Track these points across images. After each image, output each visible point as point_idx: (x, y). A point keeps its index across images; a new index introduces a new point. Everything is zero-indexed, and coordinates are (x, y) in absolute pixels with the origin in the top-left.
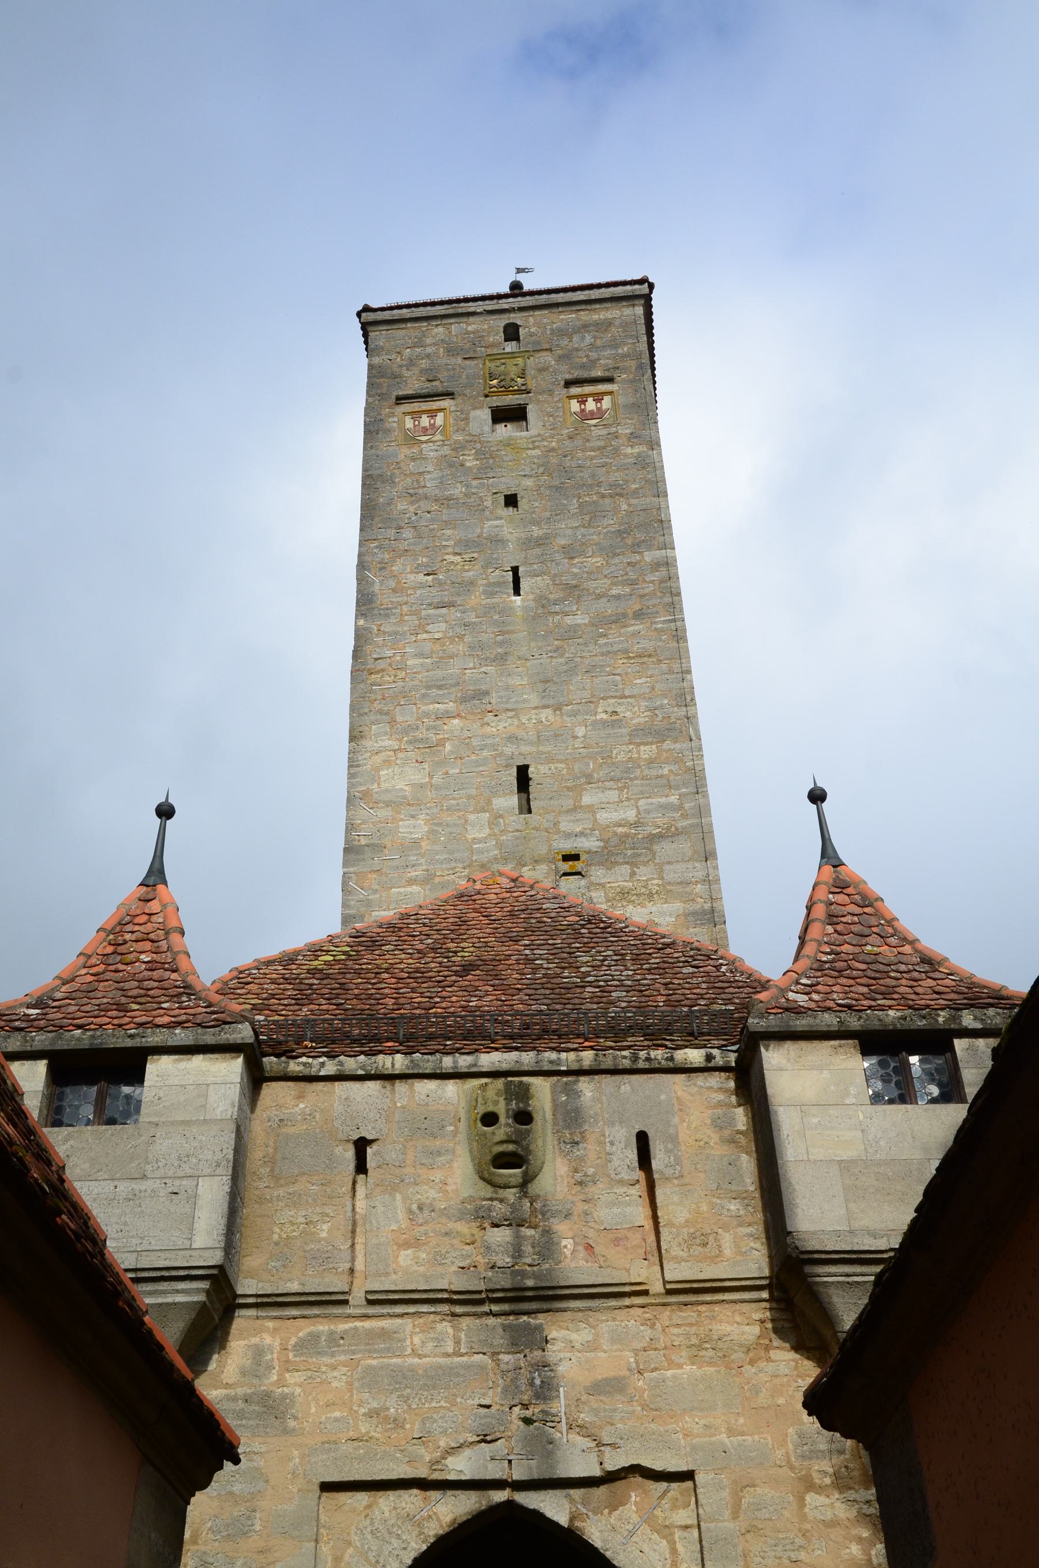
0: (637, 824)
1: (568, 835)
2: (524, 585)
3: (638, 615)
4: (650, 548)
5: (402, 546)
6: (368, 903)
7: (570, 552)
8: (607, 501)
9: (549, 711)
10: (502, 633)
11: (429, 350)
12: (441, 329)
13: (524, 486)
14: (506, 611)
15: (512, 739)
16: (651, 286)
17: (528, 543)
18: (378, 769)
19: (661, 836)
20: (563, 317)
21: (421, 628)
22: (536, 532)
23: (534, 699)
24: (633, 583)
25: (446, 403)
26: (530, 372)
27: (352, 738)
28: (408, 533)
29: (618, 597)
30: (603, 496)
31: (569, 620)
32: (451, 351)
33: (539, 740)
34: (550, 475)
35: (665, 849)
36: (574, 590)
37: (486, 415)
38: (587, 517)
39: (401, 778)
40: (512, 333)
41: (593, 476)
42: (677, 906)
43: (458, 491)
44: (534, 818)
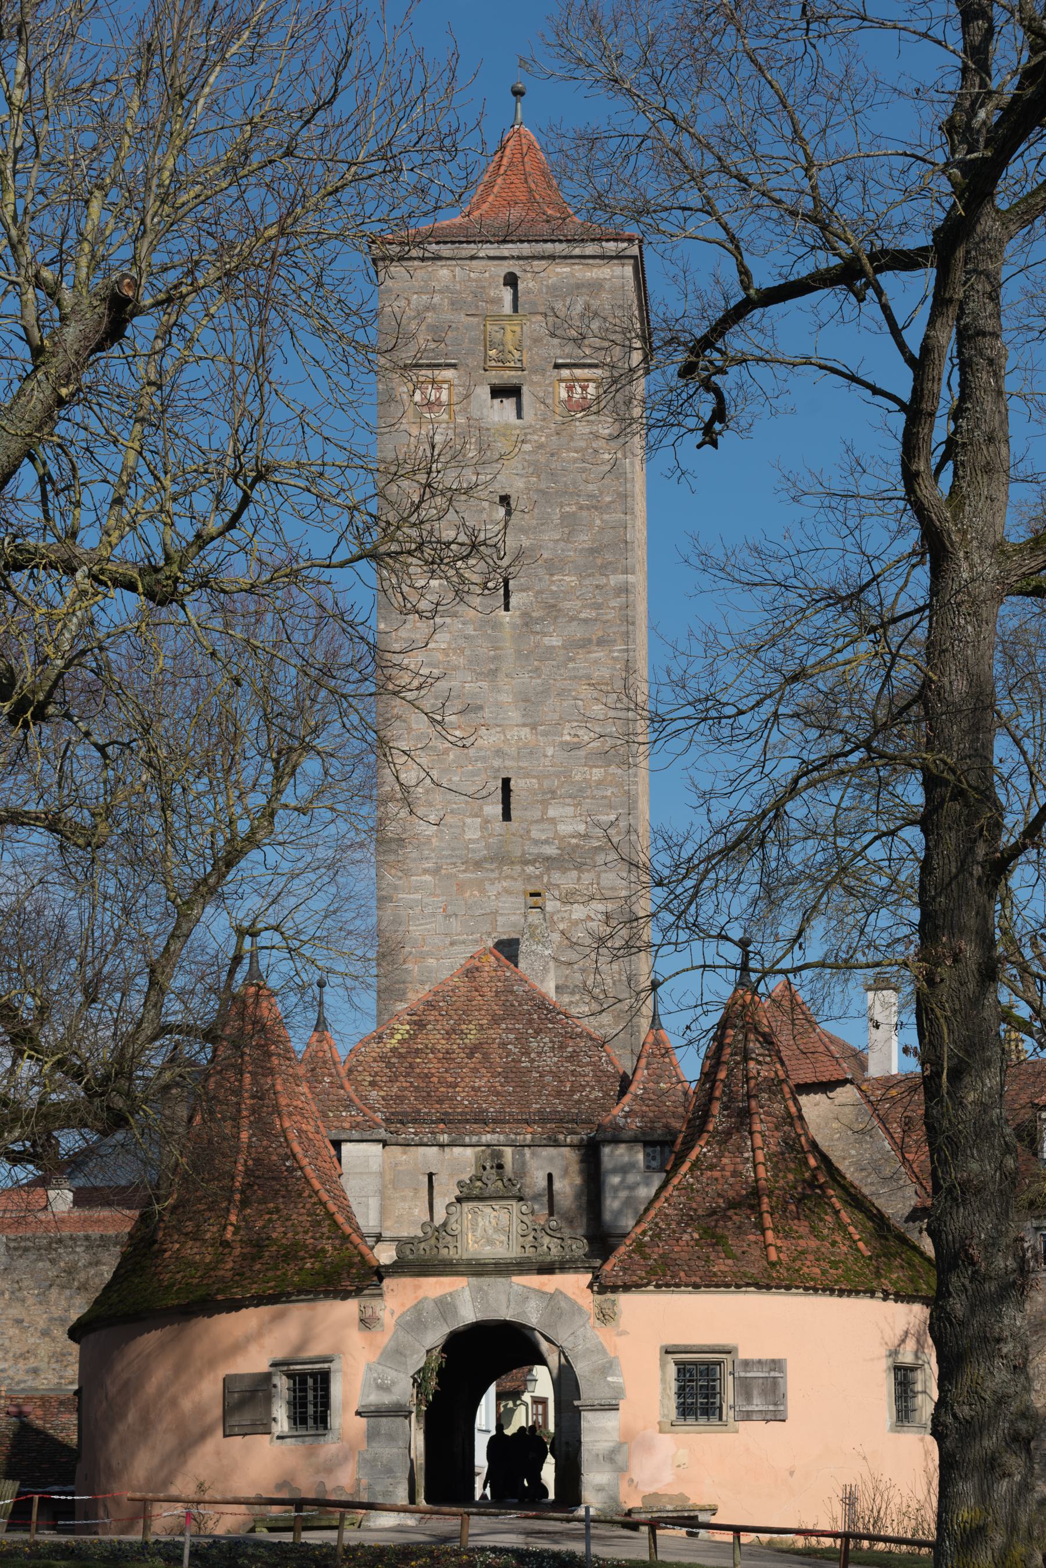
1: (536, 842)
2: (513, 601)
3: (601, 642)
4: (615, 571)
6: (396, 888)
7: (552, 567)
8: (585, 513)
9: (527, 730)
10: (496, 649)
14: (497, 625)
15: (499, 753)
20: (558, 270)
24: (597, 607)
25: (449, 374)
26: (527, 342)
30: (581, 508)
31: (547, 641)
33: (519, 757)
34: (538, 477)
36: (553, 610)
37: (485, 392)
38: (566, 531)
41: (574, 483)
44: (513, 825)
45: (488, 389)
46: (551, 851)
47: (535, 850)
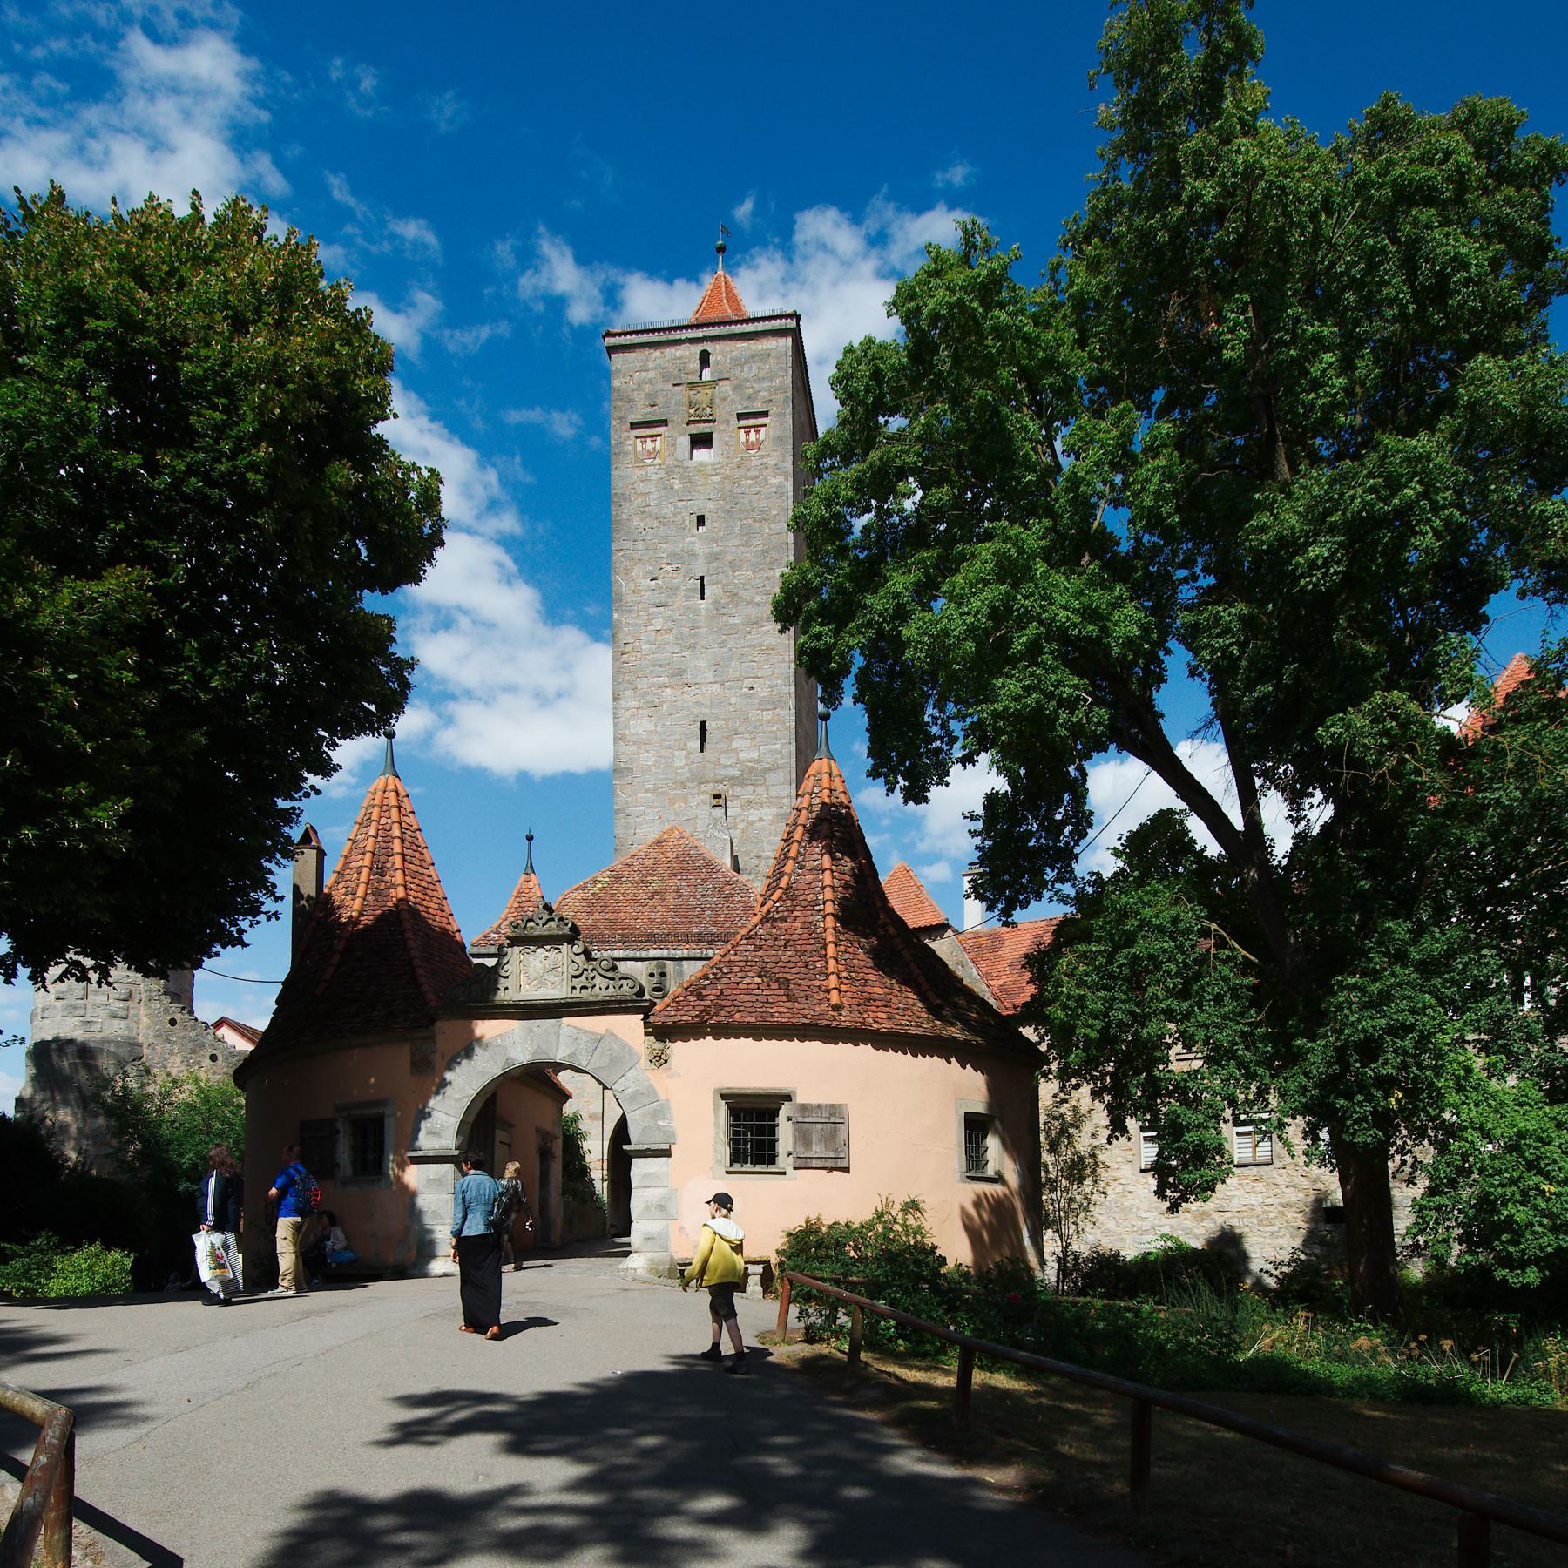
0: (759, 761)
5: (637, 555)
11: (651, 374)
12: (657, 353)
13: (708, 509)
14: (696, 611)
15: (698, 703)
16: (798, 318)
17: (713, 558)
18: (628, 720)
19: (769, 769)
21: (648, 623)
22: (716, 549)
23: (709, 676)
27: (615, 699)
28: (640, 545)
29: (758, 604)
31: (731, 620)
32: (665, 377)
35: (771, 777)
39: (641, 727)
40: (704, 359)
42: (774, 811)
43: (668, 511)
45: (688, 438)
46: (735, 772)
47: (723, 772)
